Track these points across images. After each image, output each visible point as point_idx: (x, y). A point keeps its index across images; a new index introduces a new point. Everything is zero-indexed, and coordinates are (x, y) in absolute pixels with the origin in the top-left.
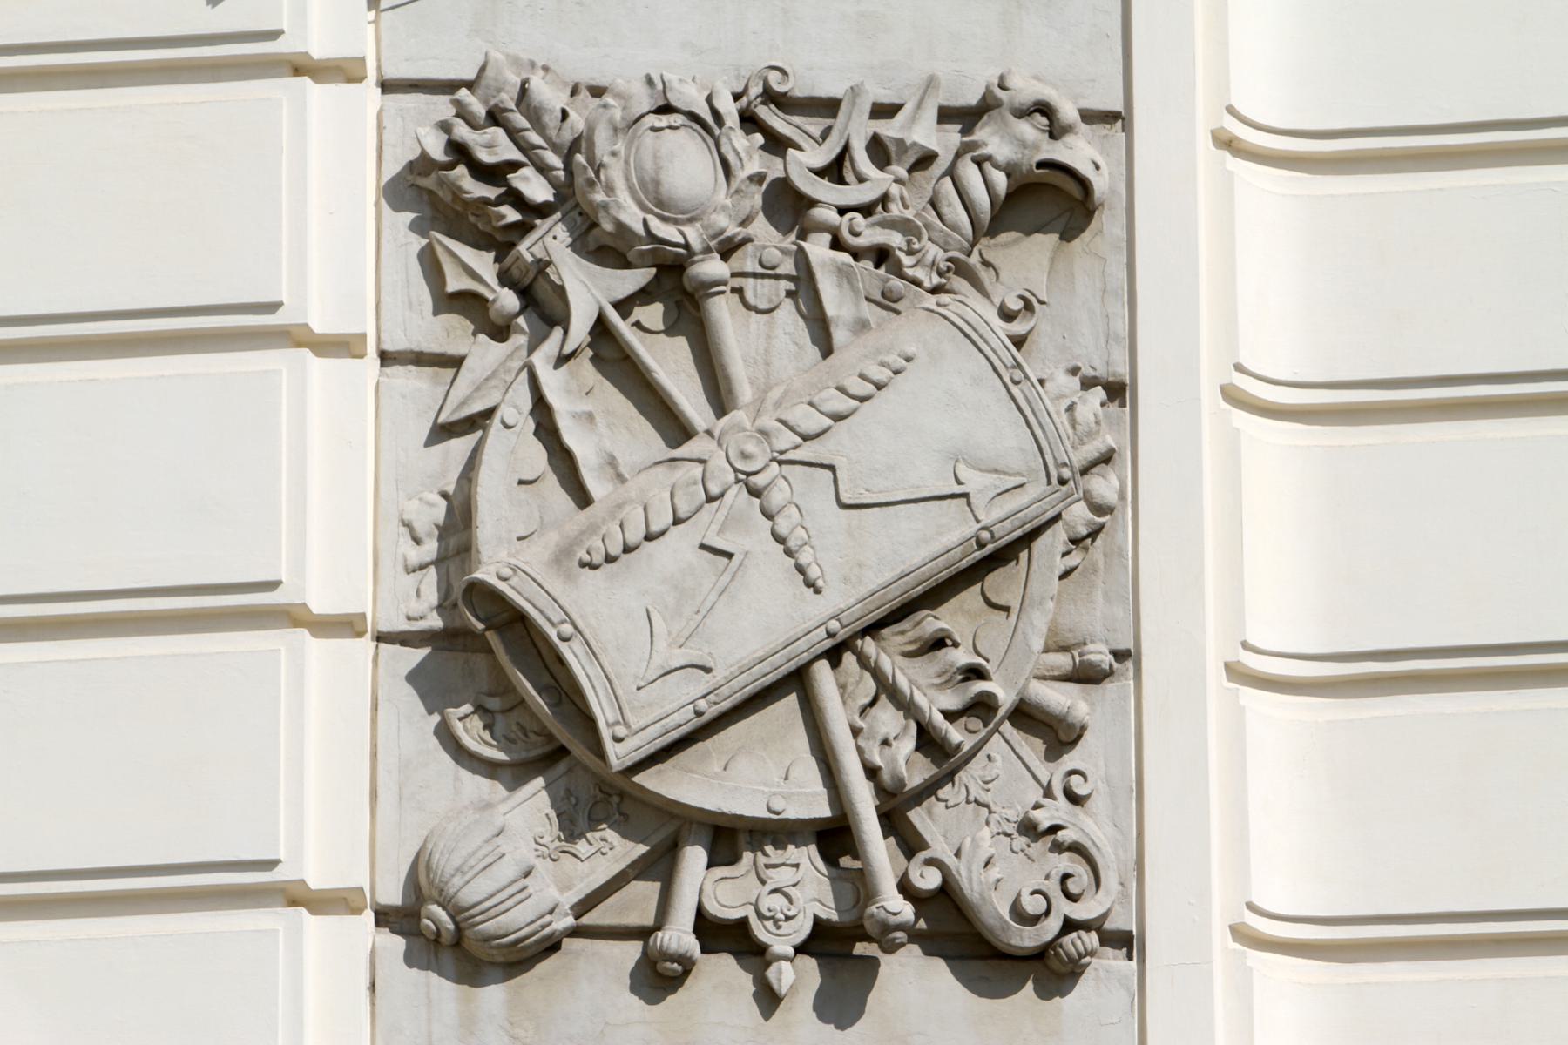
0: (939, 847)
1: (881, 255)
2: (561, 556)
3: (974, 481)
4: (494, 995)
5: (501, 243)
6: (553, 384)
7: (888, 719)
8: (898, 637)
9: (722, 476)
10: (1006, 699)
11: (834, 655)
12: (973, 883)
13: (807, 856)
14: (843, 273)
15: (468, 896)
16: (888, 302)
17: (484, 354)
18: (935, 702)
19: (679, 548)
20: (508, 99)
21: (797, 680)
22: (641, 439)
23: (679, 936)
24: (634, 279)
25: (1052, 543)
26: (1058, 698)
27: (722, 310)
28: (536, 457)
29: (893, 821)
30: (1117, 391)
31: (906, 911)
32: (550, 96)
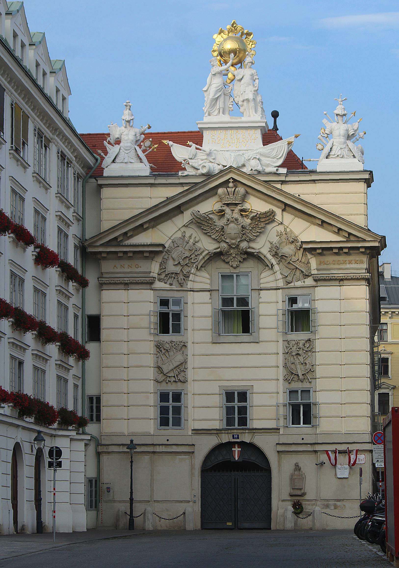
0: (179, 377)
1: (177, 349)
2: (162, 364)
3: (181, 360)
4: (159, 383)
5: (159, 349)
6: (162, 356)
7: (177, 371)
8: (177, 368)
9: (169, 360)
10: (182, 370)
11: (174, 369)
12: (180, 379)
13: (173, 377)
14: (175, 350)
15: (158, 380)
16: (177, 351)
17: (159, 354)
18: (179, 371)
19: (167, 364)
20: (160, 342)
21: (173, 369)
22: (166, 358)
23: (167, 381)
24: (165, 351)
25: (184, 363)
26: (185, 370)
27: (169, 352)
28: (161, 359)
29: (177, 376)
30: (187, 355)
31: (177, 380)
32: (161, 342)
